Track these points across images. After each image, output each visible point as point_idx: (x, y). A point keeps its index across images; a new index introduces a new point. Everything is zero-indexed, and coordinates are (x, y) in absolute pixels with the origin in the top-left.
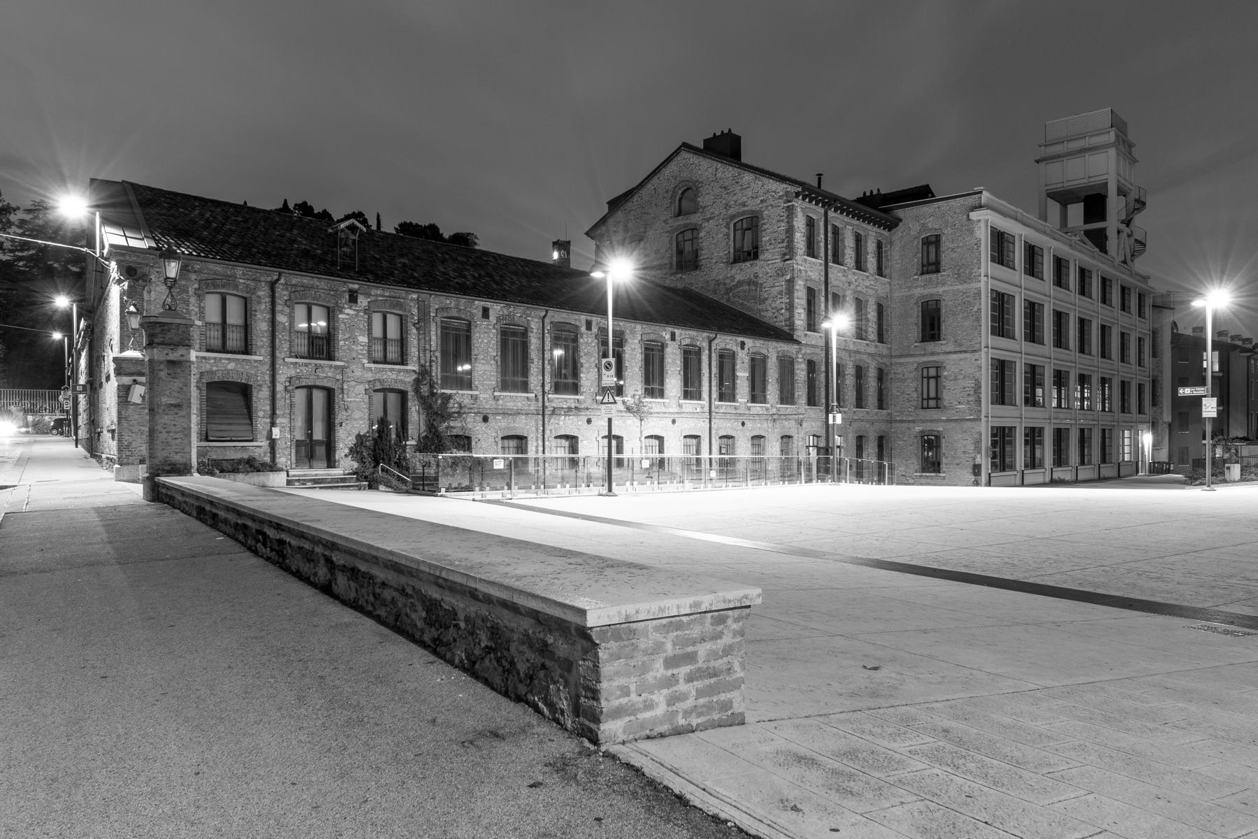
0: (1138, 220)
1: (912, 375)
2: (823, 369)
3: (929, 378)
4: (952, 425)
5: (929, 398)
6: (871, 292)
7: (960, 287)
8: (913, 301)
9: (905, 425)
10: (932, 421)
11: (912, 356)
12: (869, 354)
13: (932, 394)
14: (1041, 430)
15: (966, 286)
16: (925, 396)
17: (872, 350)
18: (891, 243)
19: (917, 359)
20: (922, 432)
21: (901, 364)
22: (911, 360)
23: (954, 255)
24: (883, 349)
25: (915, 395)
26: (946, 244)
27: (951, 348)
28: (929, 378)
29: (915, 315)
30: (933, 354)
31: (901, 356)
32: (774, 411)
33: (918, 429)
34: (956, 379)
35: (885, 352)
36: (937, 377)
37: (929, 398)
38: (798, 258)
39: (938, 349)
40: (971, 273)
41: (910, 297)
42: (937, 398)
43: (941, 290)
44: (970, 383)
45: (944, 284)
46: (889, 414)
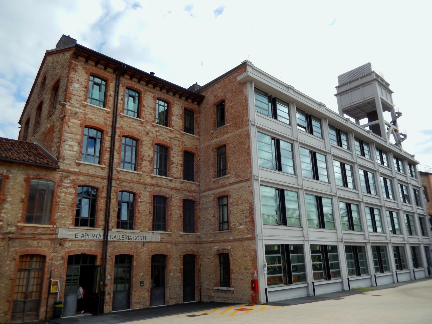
0: (398, 120)
1: (211, 205)
2: (104, 194)
3: (223, 206)
4: (236, 244)
5: (223, 222)
6: (176, 142)
7: (237, 132)
8: (211, 149)
9: (208, 245)
10: (224, 241)
11: (211, 189)
12: (172, 188)
13: (226, 220)
14: (334, 248)
15: (240, 130)
16: (221, 221)
17: (177, 184)
18: (199, 113)
19: (214, 191)
20: (218, 250)
21: (205, 196)
22: (211, 192)
23: (232, 111)
24: (189, 184)
25: (213, 220)
26: (228, 105)
27: (232, 180)
28: (223, 206)
29: (212, 158)
30: (223, 186)
31: (205, 191)
32: (13, 229)
33: (216, 248)
34: (237, 204)
35: (193, 187)
36: (227, 205)
37: (223, 222)
38: (73, 102)
39: (226, 182)
40: (242, 120)
41: (209, 146)
42: (228, 222)
43: (226, 137)
44: (246, 206)
45: (227, 133)
46: (199, 237)
